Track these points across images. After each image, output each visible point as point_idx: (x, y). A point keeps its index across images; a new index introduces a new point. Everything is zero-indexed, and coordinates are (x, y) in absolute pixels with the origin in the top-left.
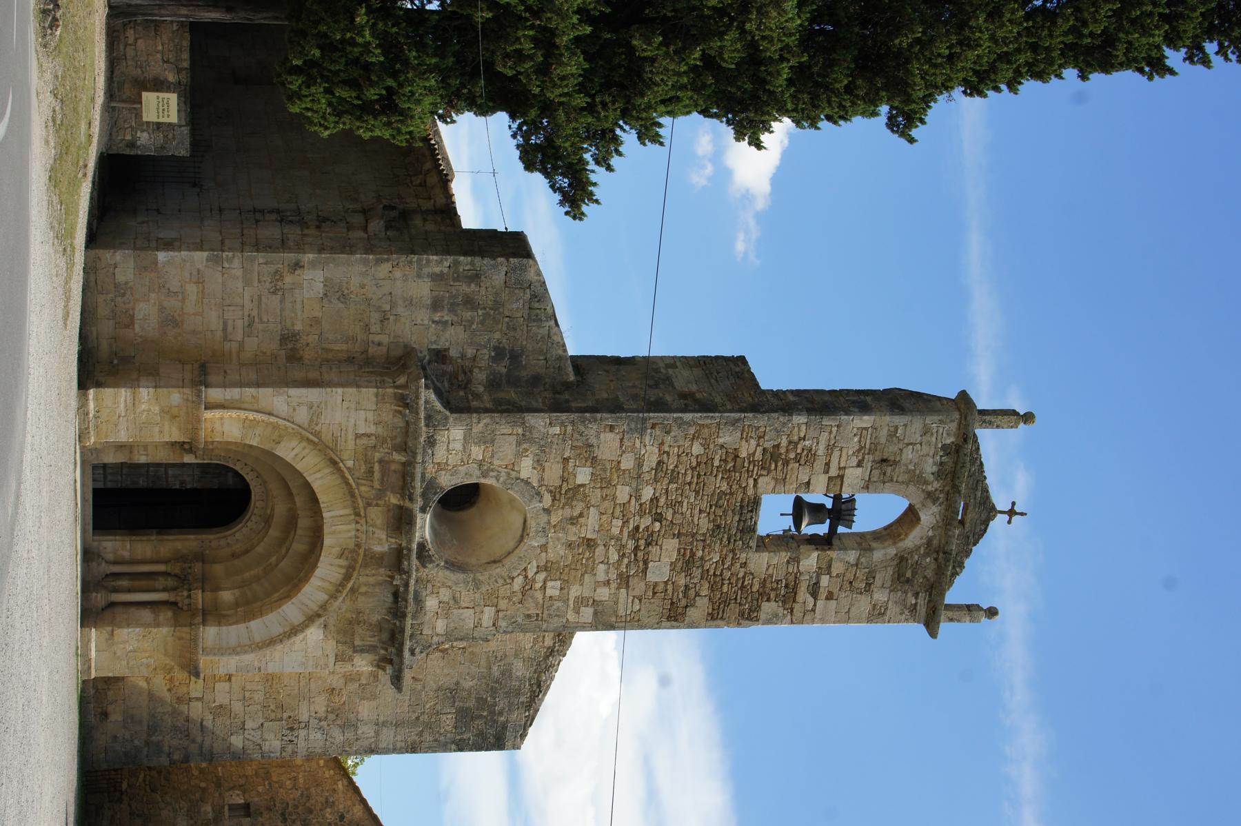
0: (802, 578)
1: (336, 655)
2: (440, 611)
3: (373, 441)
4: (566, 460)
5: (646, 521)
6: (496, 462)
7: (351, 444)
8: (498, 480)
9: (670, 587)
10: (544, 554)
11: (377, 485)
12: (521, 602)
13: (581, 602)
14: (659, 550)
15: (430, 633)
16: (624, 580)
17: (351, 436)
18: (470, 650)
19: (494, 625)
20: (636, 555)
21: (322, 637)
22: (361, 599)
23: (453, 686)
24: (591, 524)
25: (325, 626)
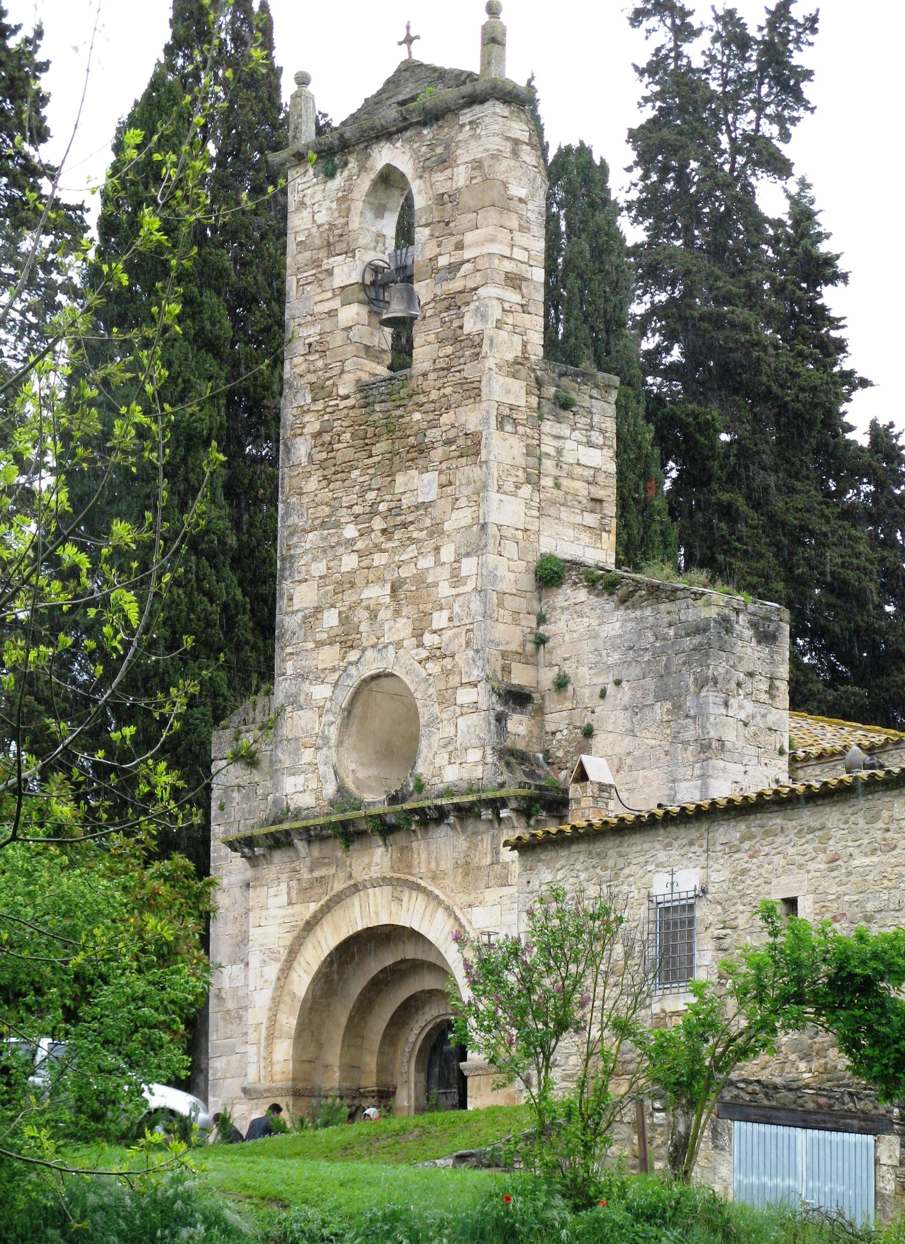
0: (439, 293)
1: (502, 886)
2: (458, 761)
3: (294, 884)
4: (319, 644)
5: (378, 524)
6: (317, 730)
7: (297, 908)
8: (333, 723)
9: (444, 466)
10: (406, 643)
11: (332, 871)
12: (453, 657)
13: (456, 579)
14: (407, 495)
15: (480, 768)
16: (436, 530)
17: (289, 911)
18: (587, 700)
19: (476, 686)
20: (412, 523)
21: (480, 908)
22: (443, 866)
23: (628, 714)
24: (378, 593)
25: (470, 906)
